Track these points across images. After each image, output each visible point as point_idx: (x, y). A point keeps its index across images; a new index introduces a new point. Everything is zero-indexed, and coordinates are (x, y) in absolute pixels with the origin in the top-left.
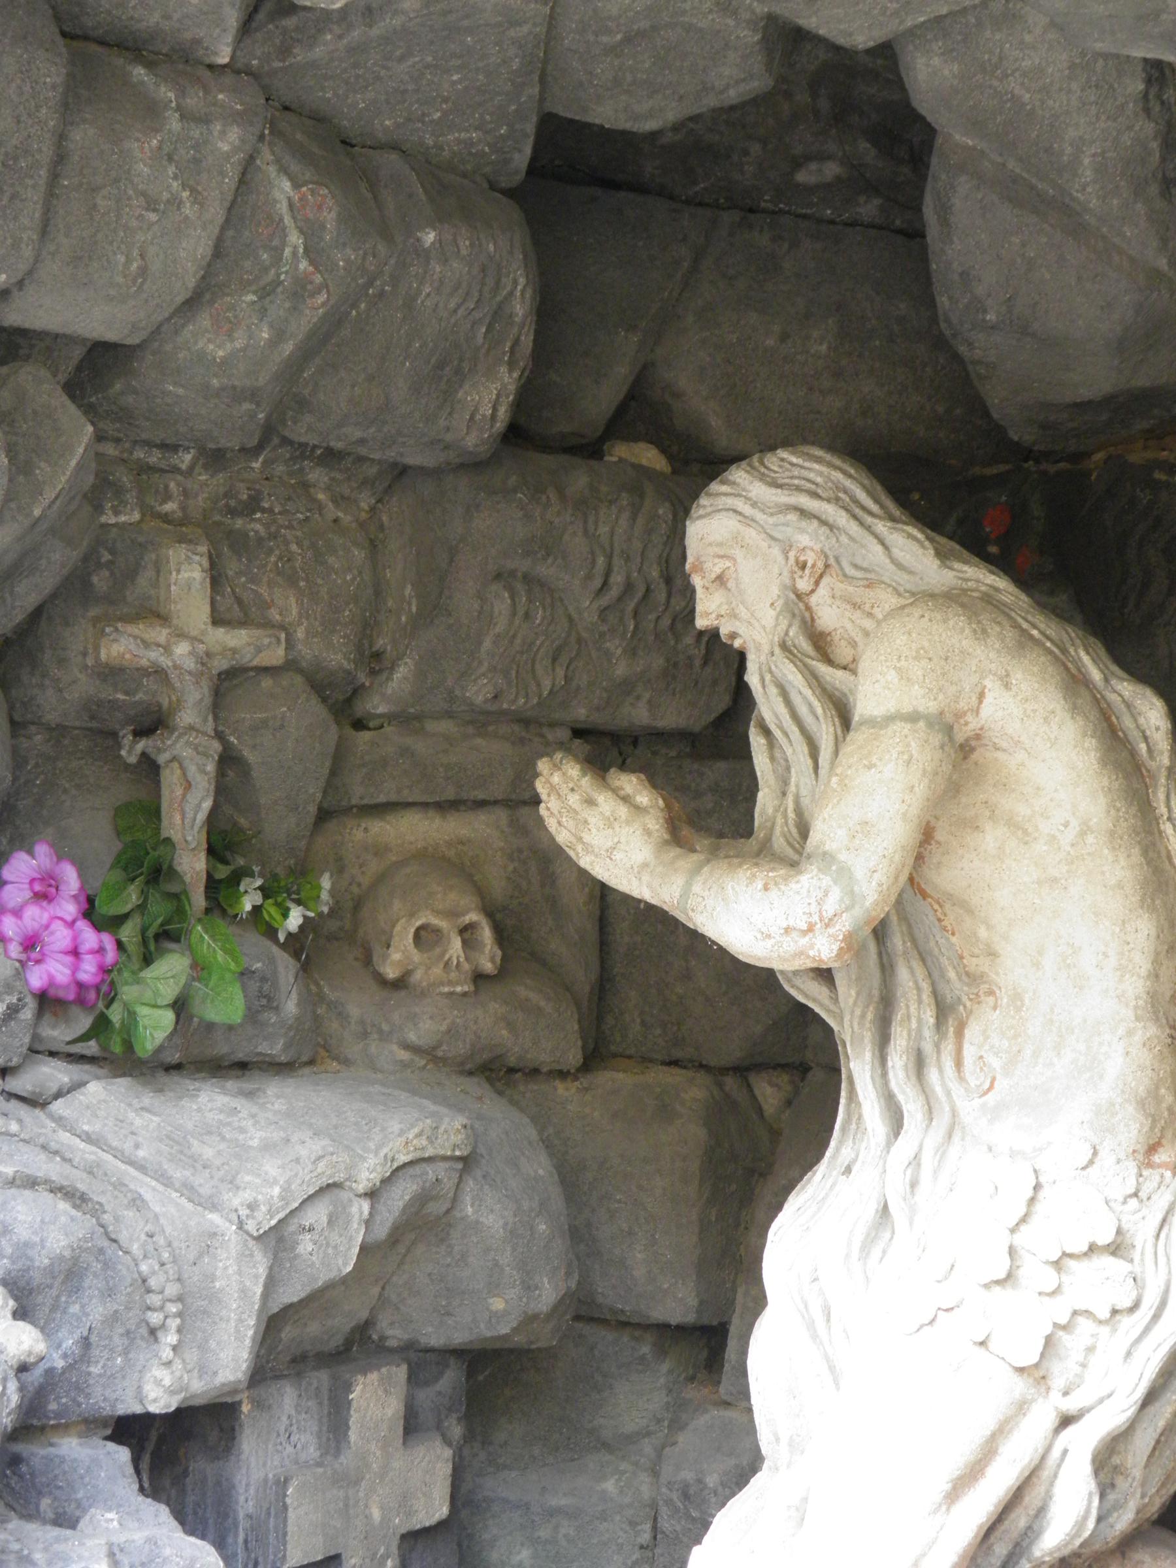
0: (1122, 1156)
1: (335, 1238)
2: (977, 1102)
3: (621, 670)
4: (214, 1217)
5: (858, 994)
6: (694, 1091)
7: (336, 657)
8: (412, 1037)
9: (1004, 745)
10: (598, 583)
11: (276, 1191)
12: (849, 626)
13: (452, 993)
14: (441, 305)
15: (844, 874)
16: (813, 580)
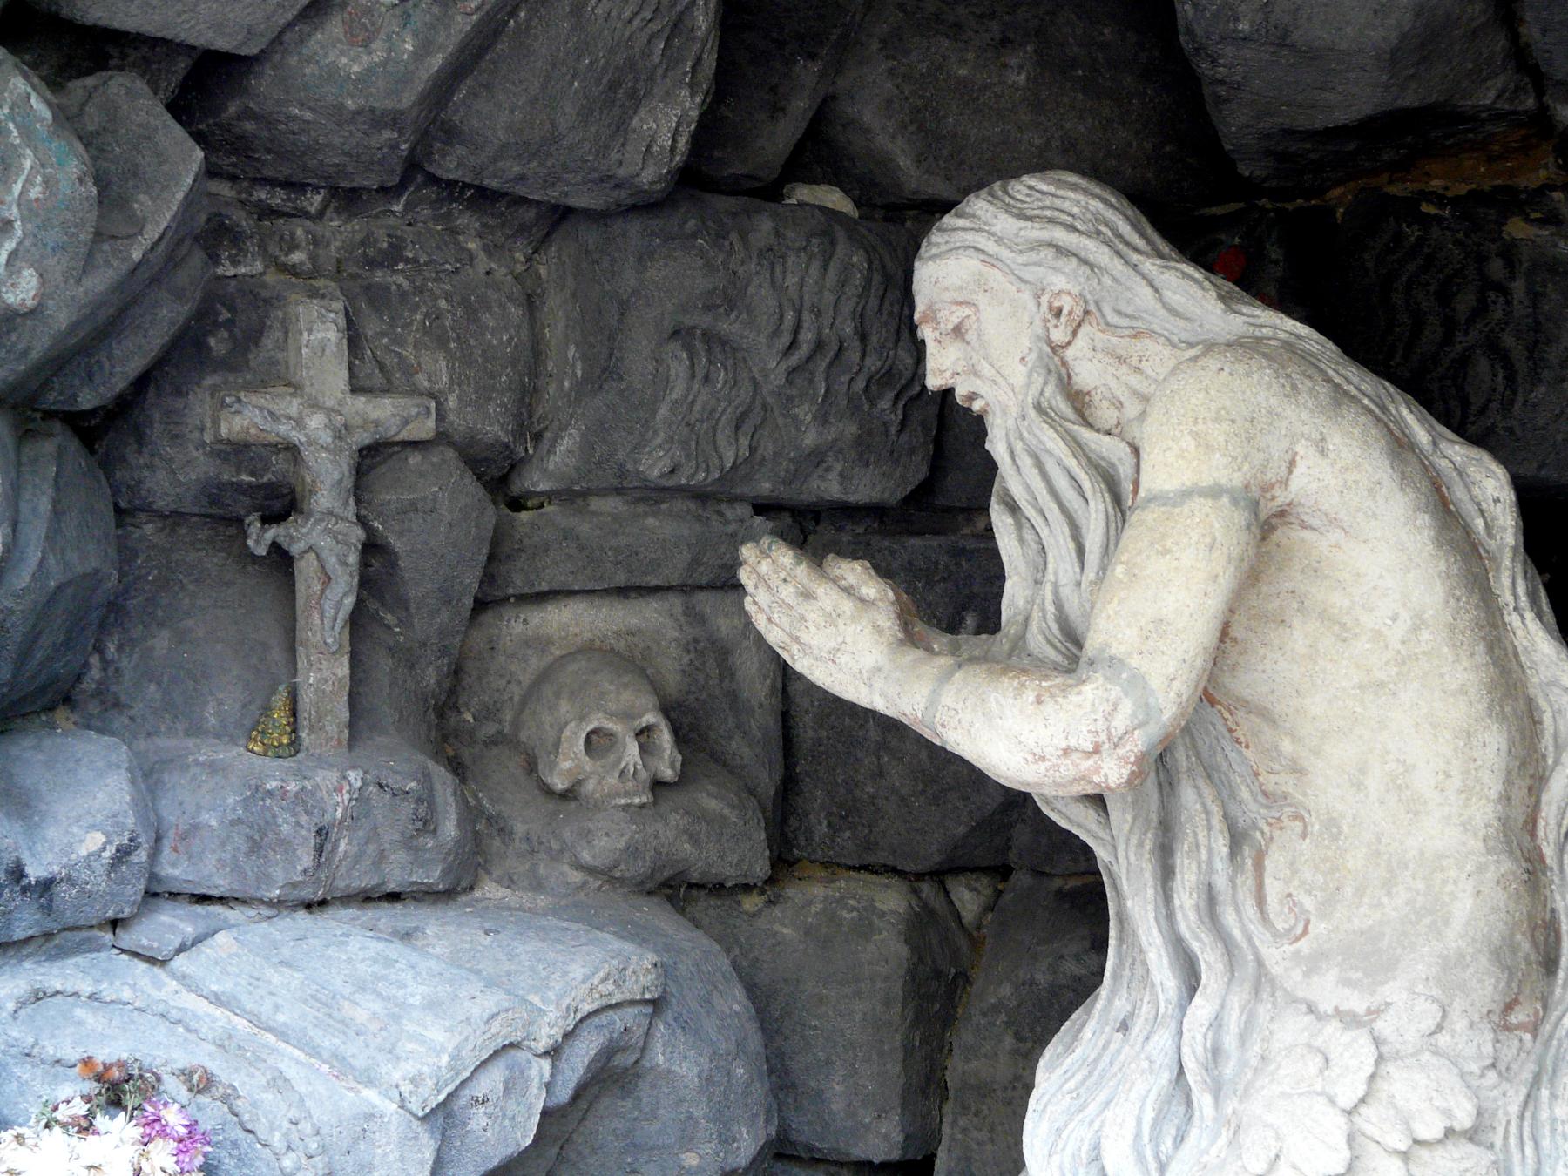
0: (1476, 1018)
1: (512, 1107)
3: (810, 439)
4: (370, 1095)
5: (1134, 819)
6: (892, 899)
7: (494, 429)
8: (586, 856)
9: (1315, 522)
10: (786, 339)
11: (445, 1059)
12: (1113, 384)
13: (629, 805)
14: (614, 13)
15: (1137, 682)
16: (1070, 330)
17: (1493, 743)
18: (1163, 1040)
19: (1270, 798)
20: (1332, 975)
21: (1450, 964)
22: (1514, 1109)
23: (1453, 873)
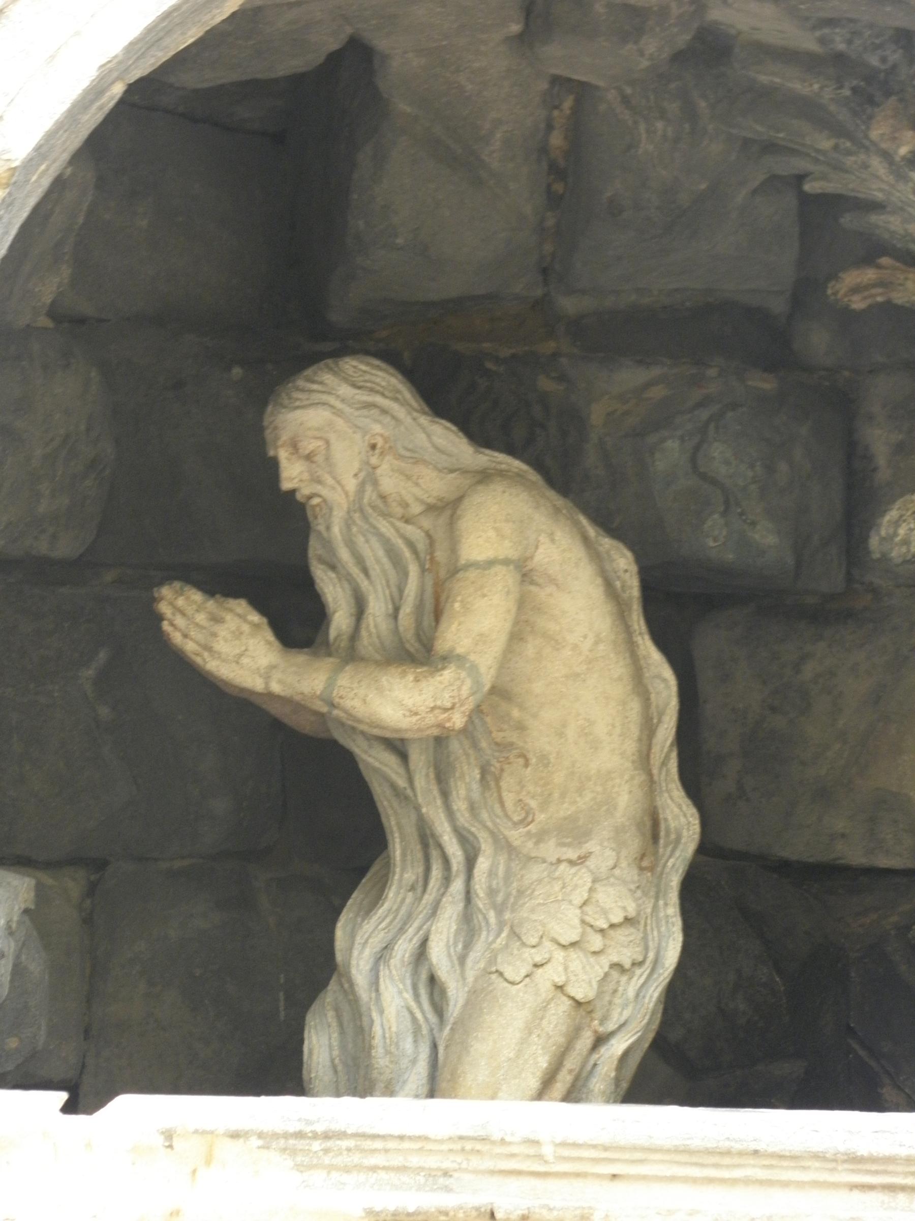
2: (523, 830)
9: (541, 581)
12: (403, 492)
17: (635, 706)
18: (458, 885)
19: (503, 747)
20: (552, 843)
21: (619, 831)
22: (649, 910)
23: (618, 781)
